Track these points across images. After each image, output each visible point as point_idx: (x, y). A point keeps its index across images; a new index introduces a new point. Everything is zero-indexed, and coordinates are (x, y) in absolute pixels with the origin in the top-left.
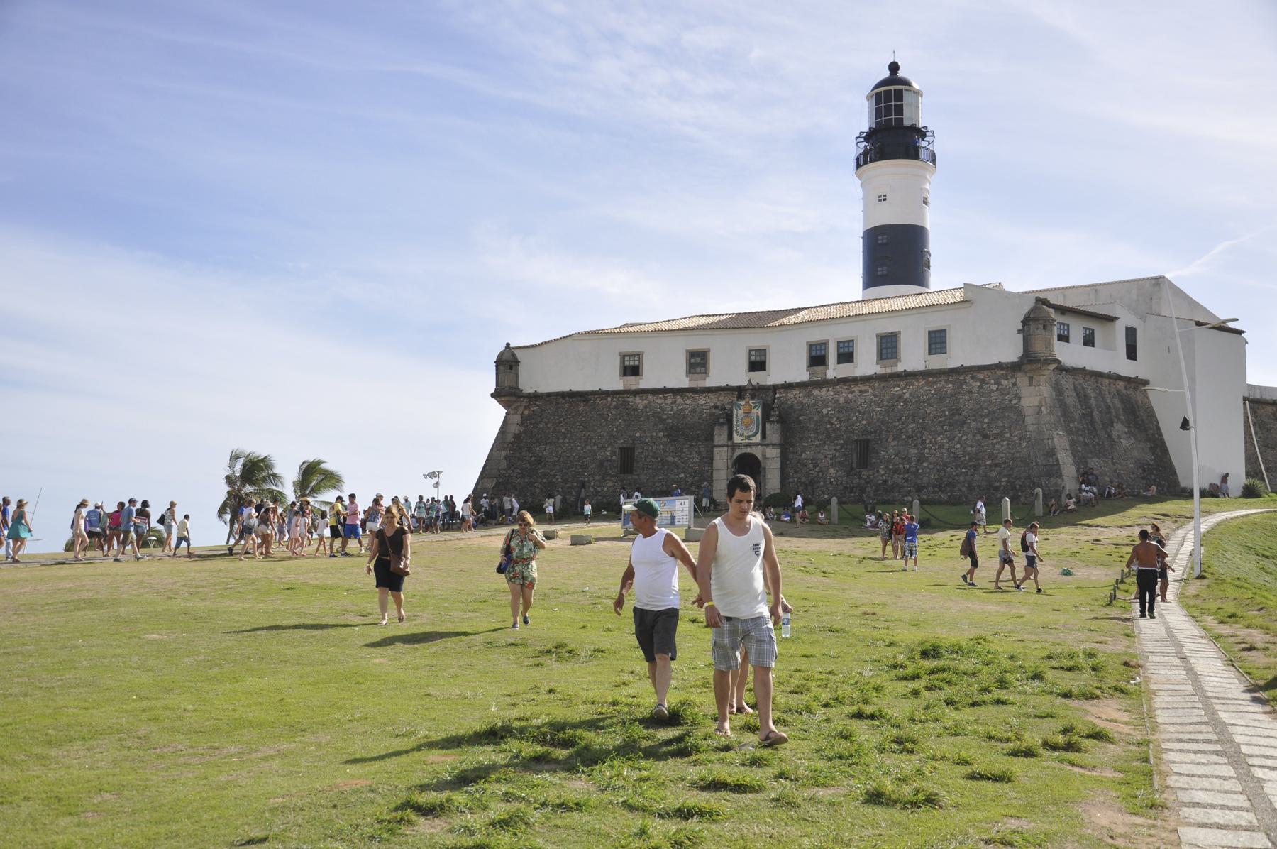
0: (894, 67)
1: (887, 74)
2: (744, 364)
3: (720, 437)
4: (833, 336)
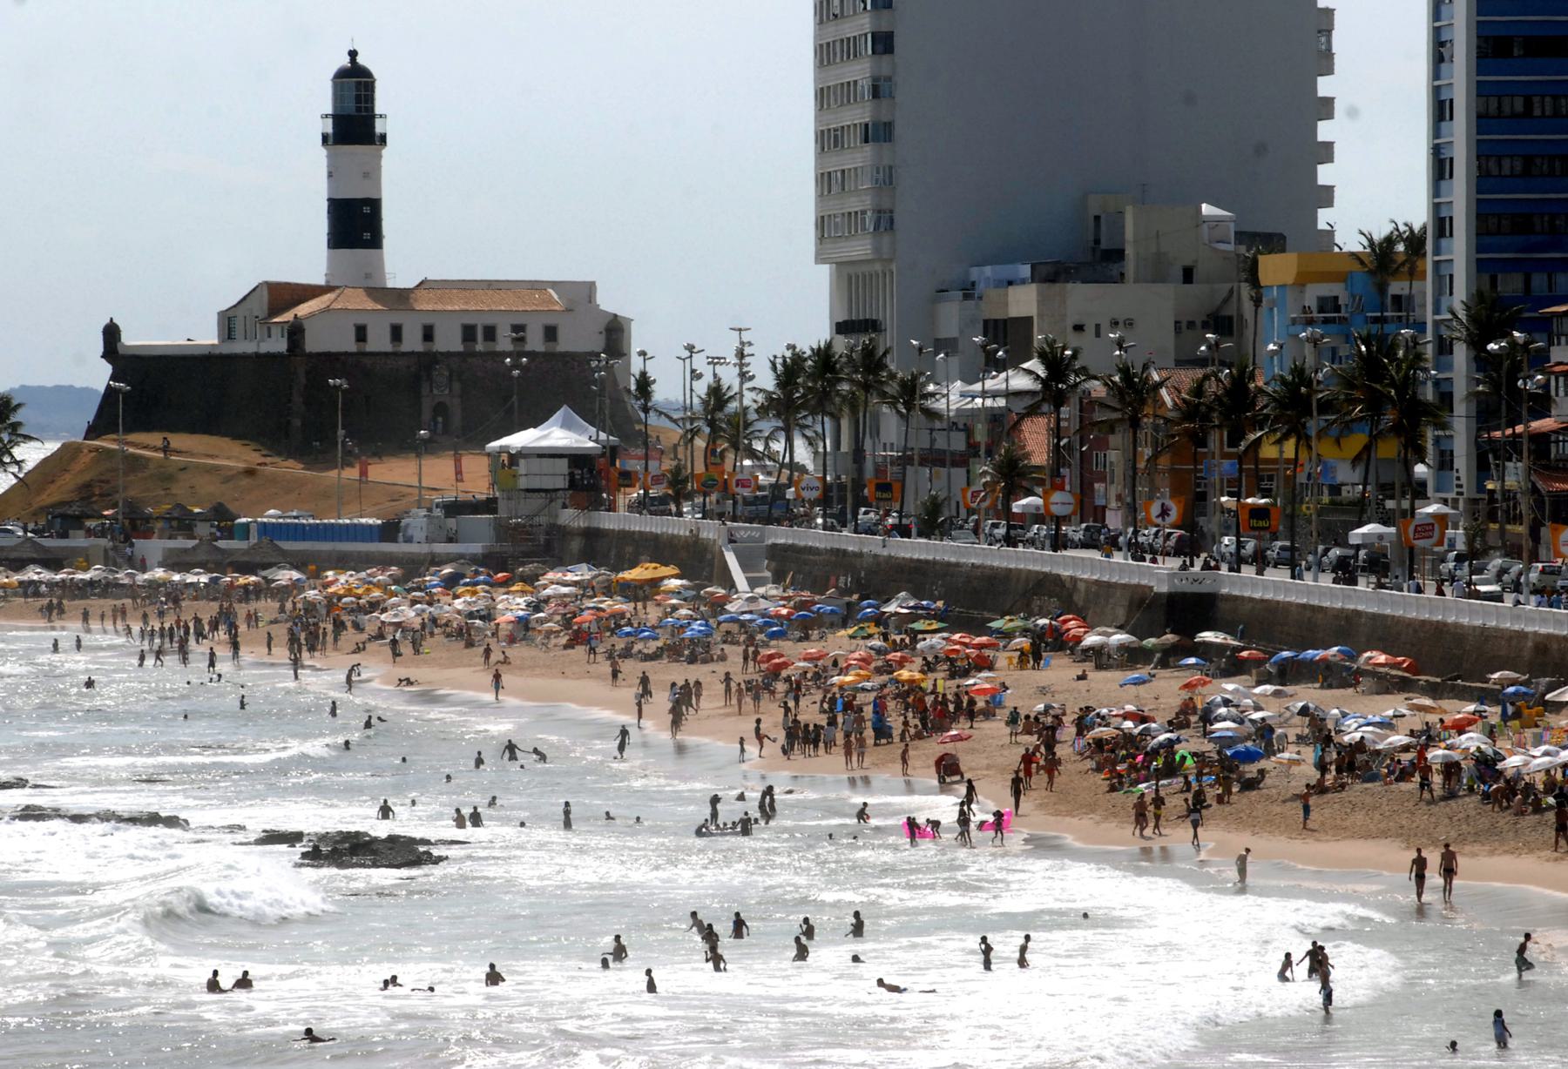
0: (353, 54)
1: (345, 61)
2: (419, 335)
3: (425, 390)
4: (480, 322)
